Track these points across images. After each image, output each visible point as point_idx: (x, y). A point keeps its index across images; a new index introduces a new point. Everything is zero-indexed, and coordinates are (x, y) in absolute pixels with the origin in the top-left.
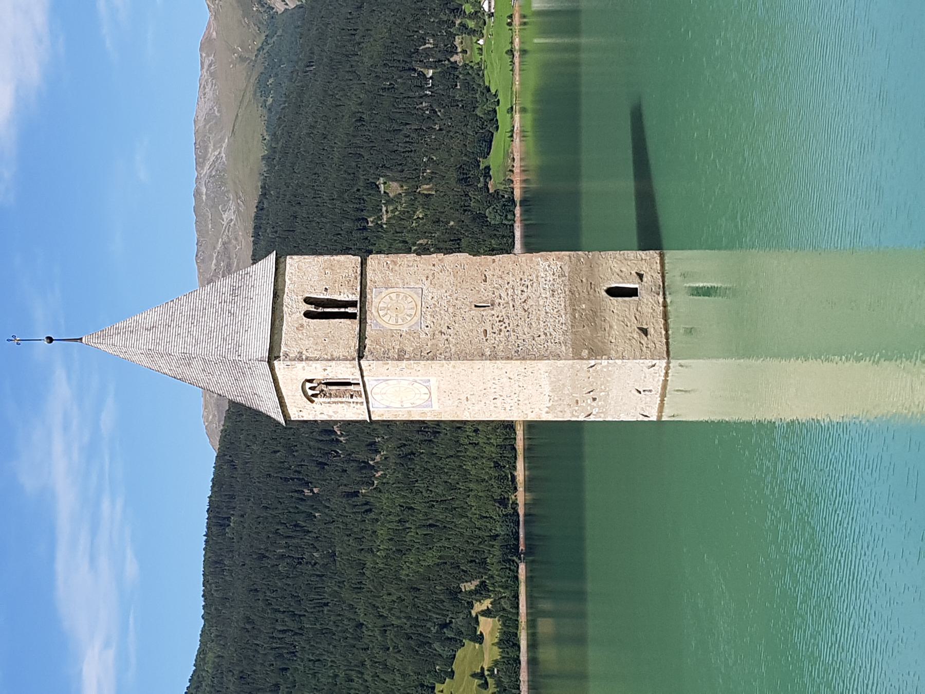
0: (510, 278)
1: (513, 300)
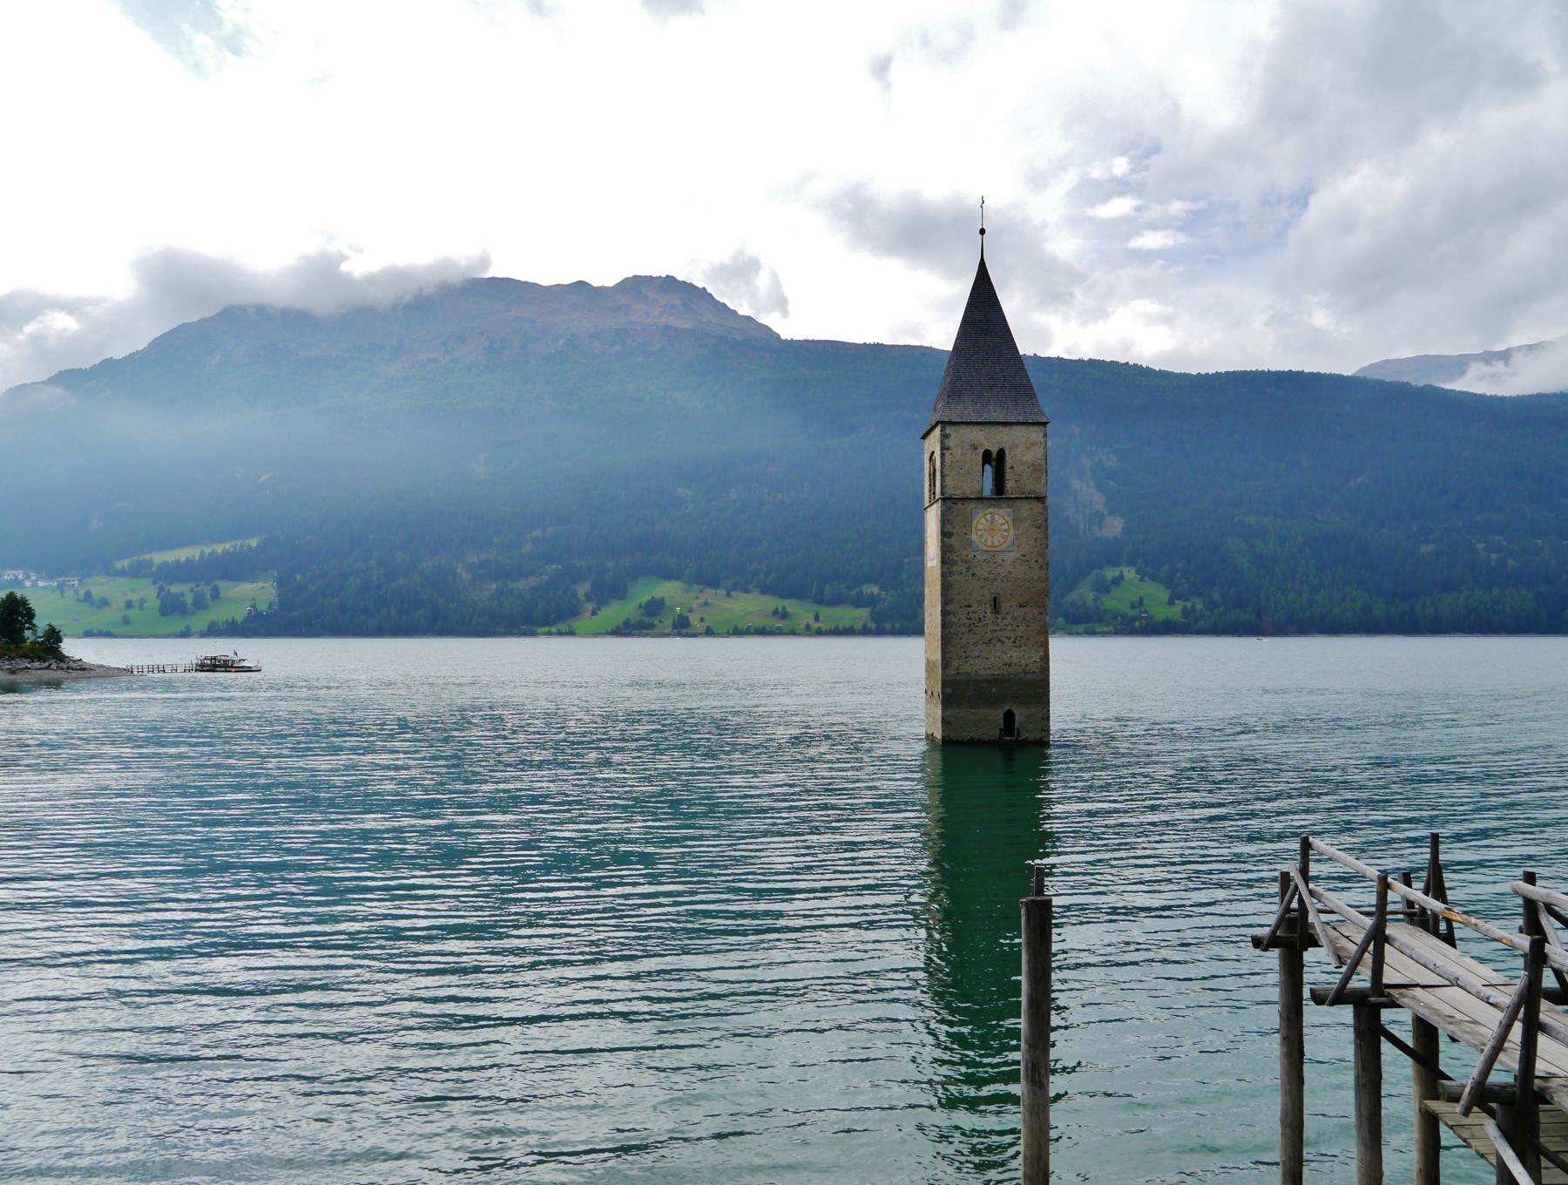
1: (1001, 630)
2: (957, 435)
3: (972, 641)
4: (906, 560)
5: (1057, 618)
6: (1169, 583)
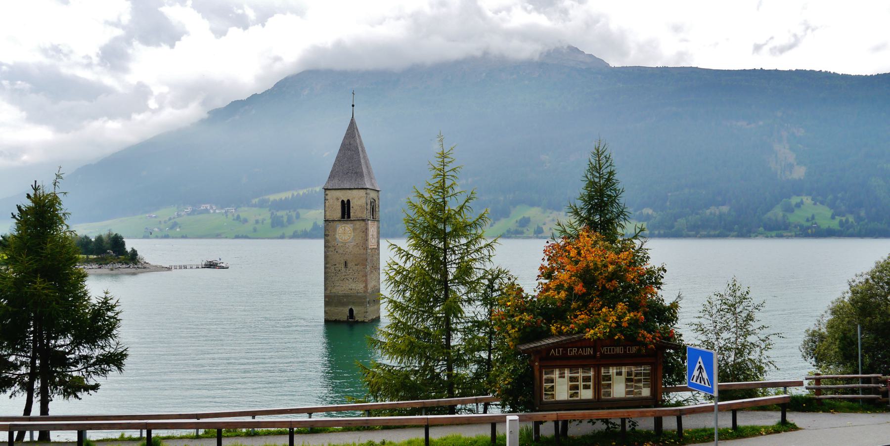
0: (356, 274)
1: (348, 275)
3: (336, 279)
4: (670, 194)
5: (759, 228)
6: (832, 206)
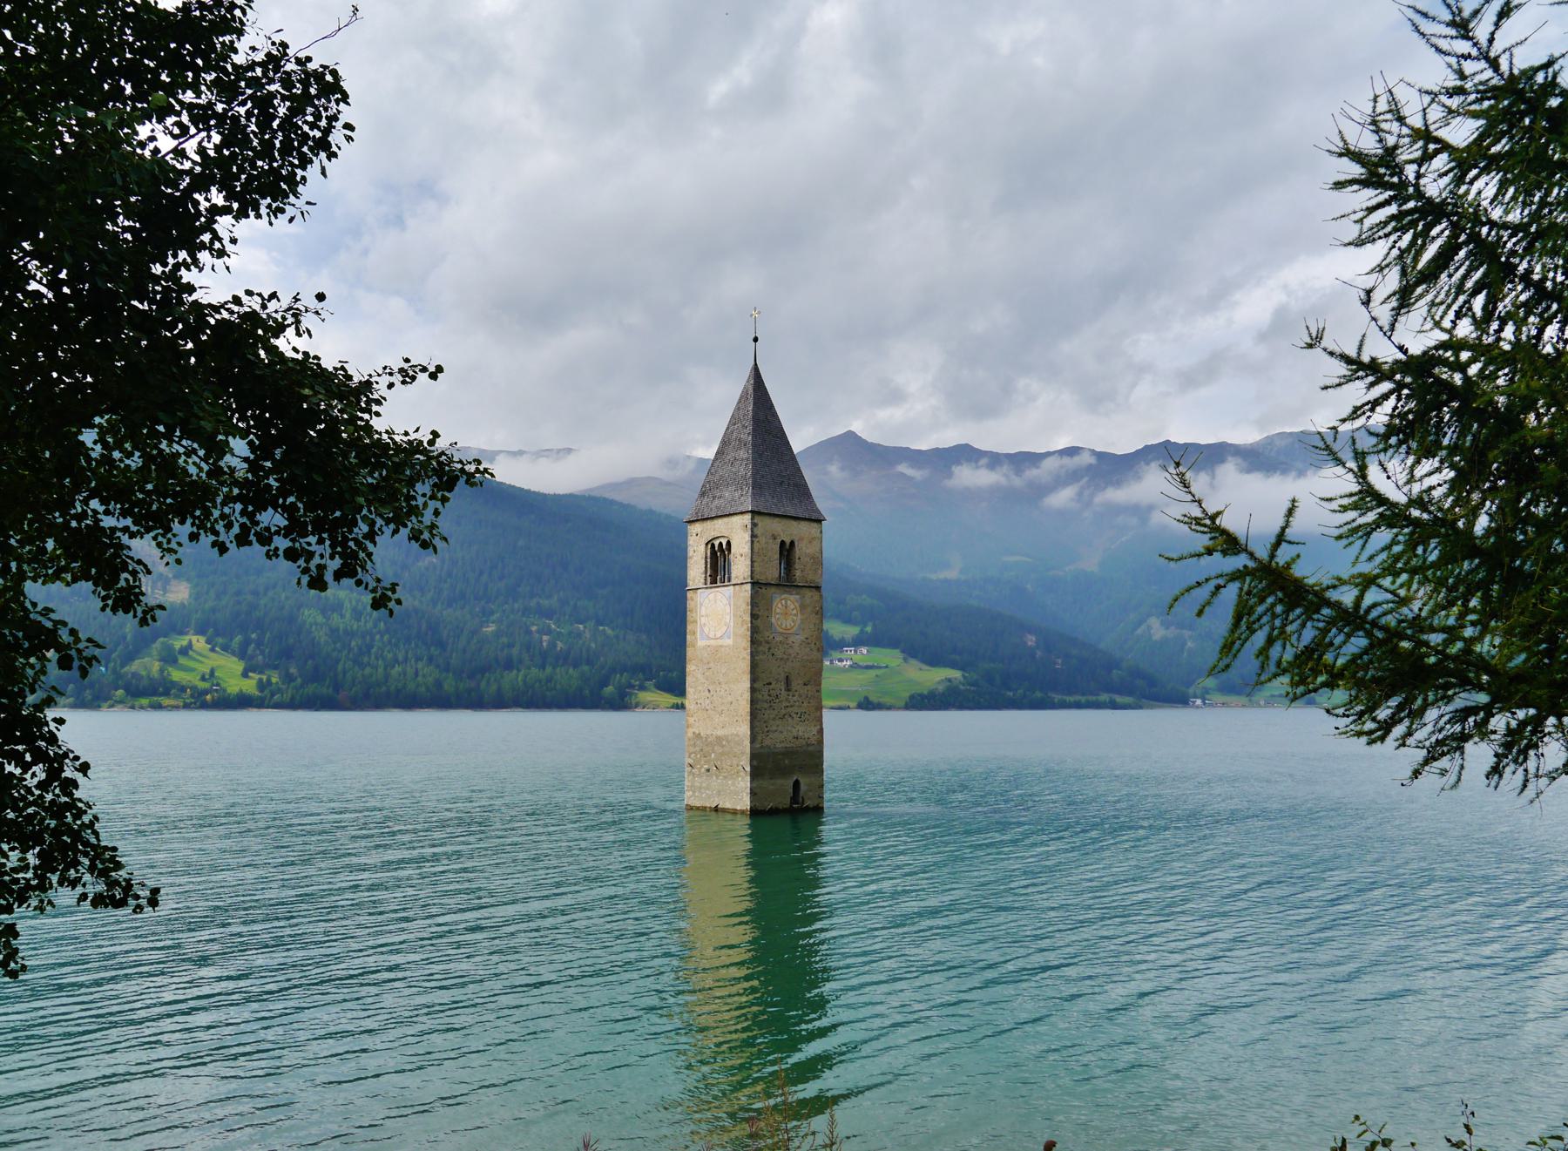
2: (766, 524)
6: (242, 654)
